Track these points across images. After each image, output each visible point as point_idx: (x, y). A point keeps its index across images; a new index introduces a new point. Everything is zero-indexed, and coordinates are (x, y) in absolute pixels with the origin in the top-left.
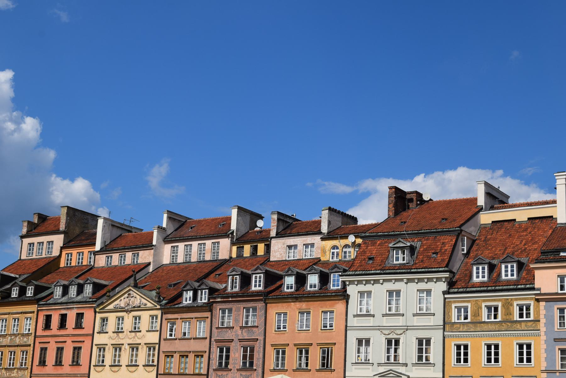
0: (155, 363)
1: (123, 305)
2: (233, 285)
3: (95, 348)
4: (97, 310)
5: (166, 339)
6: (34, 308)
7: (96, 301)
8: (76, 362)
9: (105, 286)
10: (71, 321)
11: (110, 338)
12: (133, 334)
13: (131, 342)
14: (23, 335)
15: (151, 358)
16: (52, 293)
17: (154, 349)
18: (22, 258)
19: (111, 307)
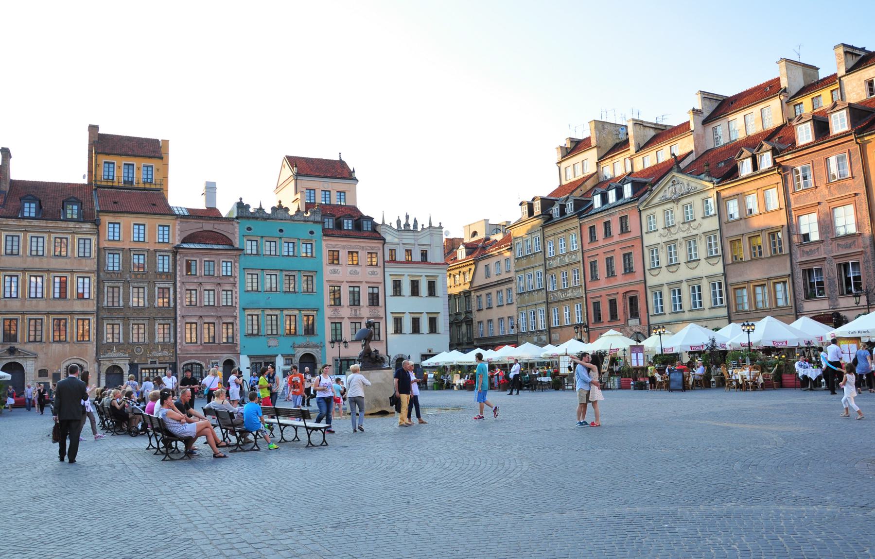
0: (720, 252)
1: (668, 196)
2: (805, 134)
3: (646, 251)
4: (641, 209)
5: (728, 222)
6: (576, 222)
7: (638, 200)
8: (629, 270)
9: (646, 183)
10: (615, 228)
11: (661, 235)
12: (687, 226)
13: (685, 235)
14: (571, 253)
15: (713, 249)
16: (592, 205)
17: (715, 237)
18: (564, 183)
19: (656, 200)
